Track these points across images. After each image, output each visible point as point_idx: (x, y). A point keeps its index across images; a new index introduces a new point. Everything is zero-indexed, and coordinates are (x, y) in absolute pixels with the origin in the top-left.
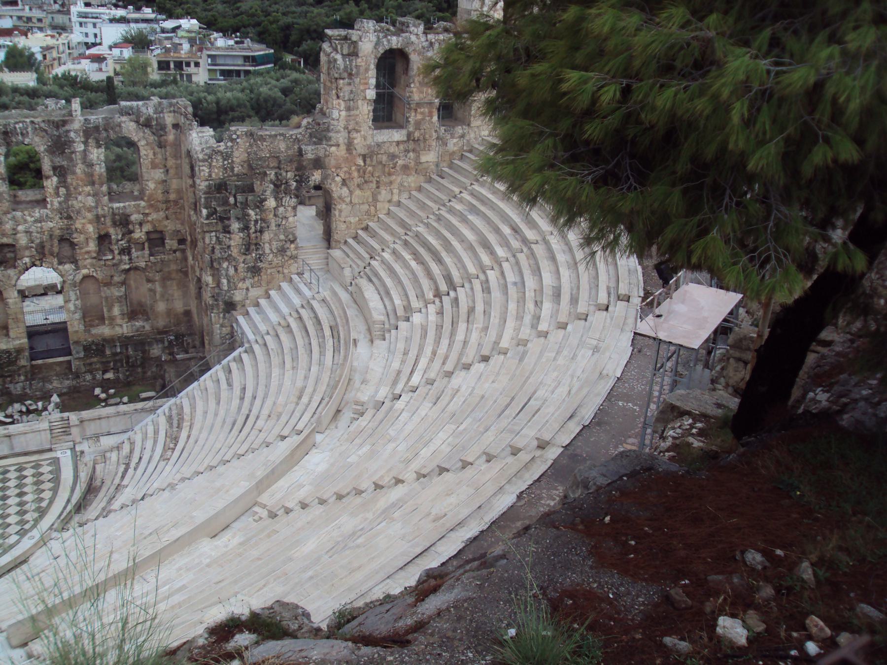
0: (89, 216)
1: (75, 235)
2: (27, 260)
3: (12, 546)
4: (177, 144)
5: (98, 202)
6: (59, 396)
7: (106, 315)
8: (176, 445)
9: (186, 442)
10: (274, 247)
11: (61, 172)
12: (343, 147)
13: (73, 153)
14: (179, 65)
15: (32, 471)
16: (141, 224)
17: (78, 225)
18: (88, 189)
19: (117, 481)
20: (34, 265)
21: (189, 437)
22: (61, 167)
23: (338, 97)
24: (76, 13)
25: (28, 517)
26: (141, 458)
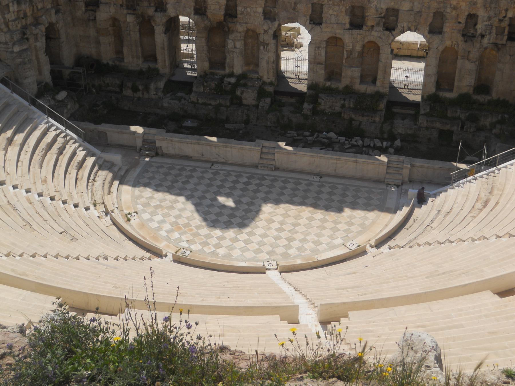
1: (448, 10)
2: (405, 24)
6: (401, 141)
7: (456, 84)
8: (484, 207)
9: (494, 208)
15: (366, 195)
16: (507, 10)
19: (427, 222)
20: (410, 29)
21: (497, 203)
25: (353, 228)
26: (451, 209)
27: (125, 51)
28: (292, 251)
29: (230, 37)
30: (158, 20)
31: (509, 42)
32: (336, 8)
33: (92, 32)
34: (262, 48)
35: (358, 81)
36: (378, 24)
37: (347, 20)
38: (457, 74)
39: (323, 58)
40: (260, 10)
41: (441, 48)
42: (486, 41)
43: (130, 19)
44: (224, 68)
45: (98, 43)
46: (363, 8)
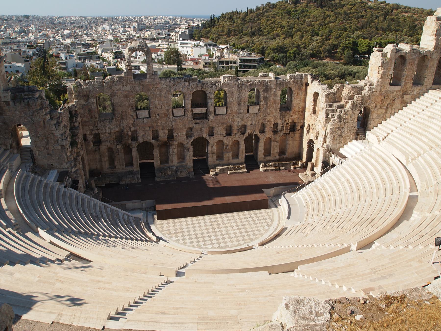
0: (272, 115)
1: (267, 122)
3: (267, 230)
4: (306, 90)
5: (276, 110)
7: (272, 152)
10: (348, 128)
11: (266, 99)
12: (378, 92)
13: (271, 92)
14: (228, 63)
16: (288, 120)
17: (268, 119)
18: (274, 105)
22: (267, 97)
23: (379, 73)
24: (180, 44)
27: (116, 163)
28: (252, 237)
29: (171, 148)
30: (134, 145)
31: (291, 133)
32: (220, 128)
33: (98, 157)
34: (186, 150)
35: (231, 158)
36: (238, 132)
37: (225, 132)
38: (272, 148)
39: (215, 151)
40: (185, 133)
41: (265, 138)
42: (282, 133)
43: (119, 147)
44: (168, 163)
45: (101, 161)
46: (231, 127)
